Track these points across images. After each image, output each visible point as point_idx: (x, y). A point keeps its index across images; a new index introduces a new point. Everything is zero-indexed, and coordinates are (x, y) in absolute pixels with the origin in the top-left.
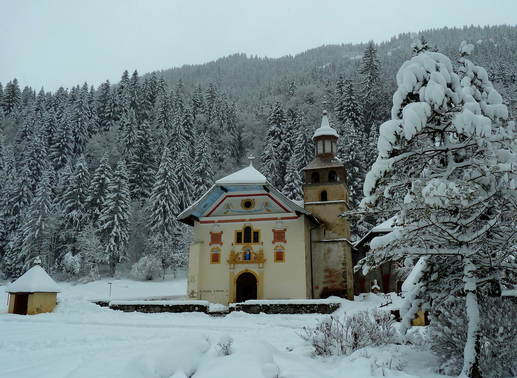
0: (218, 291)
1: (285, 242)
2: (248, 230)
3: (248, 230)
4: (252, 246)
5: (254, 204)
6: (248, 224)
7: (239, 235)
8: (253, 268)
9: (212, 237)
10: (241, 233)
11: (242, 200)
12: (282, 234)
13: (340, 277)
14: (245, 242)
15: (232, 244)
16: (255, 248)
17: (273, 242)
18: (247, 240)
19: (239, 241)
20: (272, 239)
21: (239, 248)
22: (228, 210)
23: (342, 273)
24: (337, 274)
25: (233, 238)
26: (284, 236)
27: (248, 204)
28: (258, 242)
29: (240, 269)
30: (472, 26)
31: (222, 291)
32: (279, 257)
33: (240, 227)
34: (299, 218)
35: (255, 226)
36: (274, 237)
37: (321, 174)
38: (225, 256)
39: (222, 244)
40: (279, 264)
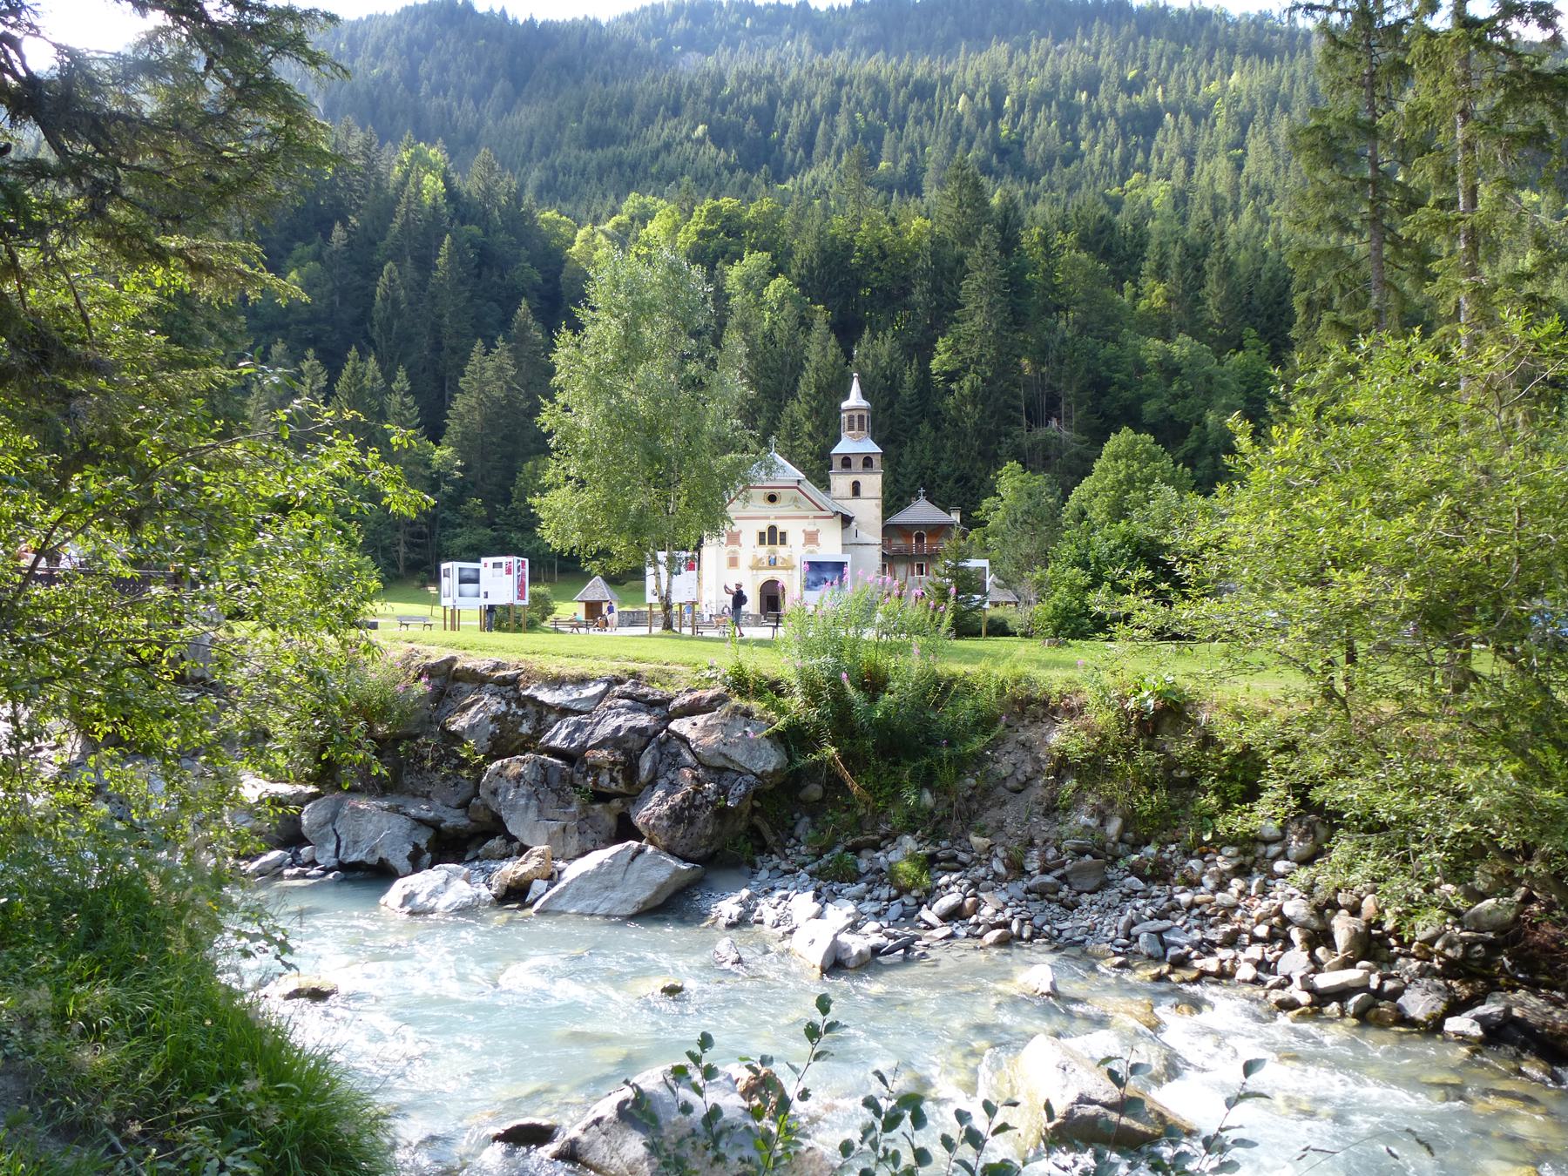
2: (772, 529)
3: (772, 529)
6: (773, 522)
7: (762, 534)
16: (781, 551)
18: (772, 541)
19: (762, 542)
21: (764, 551)
27: (772, 499)
33: (763, 526)
35: (781, 526)
37: (853, 460)
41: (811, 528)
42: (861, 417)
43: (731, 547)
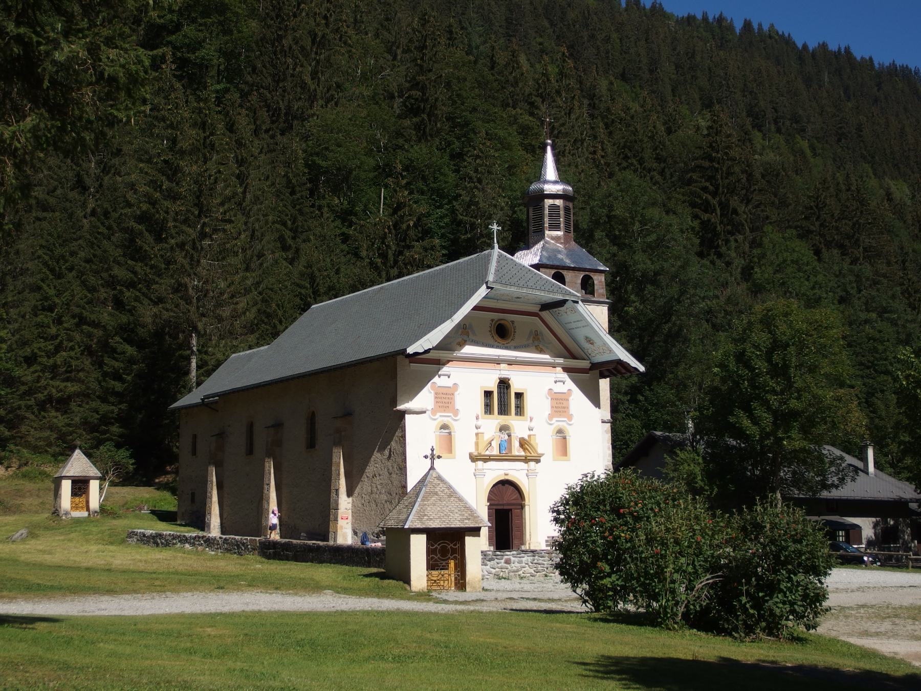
1: (570, 417)
2: (504, 384)
3: (504, 384)
4: (513, 422)
5: (515, 332)
7: (488, 394)
8: (516, 472)
9: (436, 398)
10: (492, 392)
11: (492, 320)
16: (519, 427)
17: (551, 417)
18: (504, 410)
19: (488, 408)
20: (548, 411)
22: (465, 337)
25: (479, 401)
29: (496, 472)
30: (824, 46)
33: (489, 379)
34: (590, 372)
35: (519, 380)
36: (552, 407)
39: (456, 412)
40: (562, 464)
41: (560, 388)
42: (567, 209)
43: (441, 418)
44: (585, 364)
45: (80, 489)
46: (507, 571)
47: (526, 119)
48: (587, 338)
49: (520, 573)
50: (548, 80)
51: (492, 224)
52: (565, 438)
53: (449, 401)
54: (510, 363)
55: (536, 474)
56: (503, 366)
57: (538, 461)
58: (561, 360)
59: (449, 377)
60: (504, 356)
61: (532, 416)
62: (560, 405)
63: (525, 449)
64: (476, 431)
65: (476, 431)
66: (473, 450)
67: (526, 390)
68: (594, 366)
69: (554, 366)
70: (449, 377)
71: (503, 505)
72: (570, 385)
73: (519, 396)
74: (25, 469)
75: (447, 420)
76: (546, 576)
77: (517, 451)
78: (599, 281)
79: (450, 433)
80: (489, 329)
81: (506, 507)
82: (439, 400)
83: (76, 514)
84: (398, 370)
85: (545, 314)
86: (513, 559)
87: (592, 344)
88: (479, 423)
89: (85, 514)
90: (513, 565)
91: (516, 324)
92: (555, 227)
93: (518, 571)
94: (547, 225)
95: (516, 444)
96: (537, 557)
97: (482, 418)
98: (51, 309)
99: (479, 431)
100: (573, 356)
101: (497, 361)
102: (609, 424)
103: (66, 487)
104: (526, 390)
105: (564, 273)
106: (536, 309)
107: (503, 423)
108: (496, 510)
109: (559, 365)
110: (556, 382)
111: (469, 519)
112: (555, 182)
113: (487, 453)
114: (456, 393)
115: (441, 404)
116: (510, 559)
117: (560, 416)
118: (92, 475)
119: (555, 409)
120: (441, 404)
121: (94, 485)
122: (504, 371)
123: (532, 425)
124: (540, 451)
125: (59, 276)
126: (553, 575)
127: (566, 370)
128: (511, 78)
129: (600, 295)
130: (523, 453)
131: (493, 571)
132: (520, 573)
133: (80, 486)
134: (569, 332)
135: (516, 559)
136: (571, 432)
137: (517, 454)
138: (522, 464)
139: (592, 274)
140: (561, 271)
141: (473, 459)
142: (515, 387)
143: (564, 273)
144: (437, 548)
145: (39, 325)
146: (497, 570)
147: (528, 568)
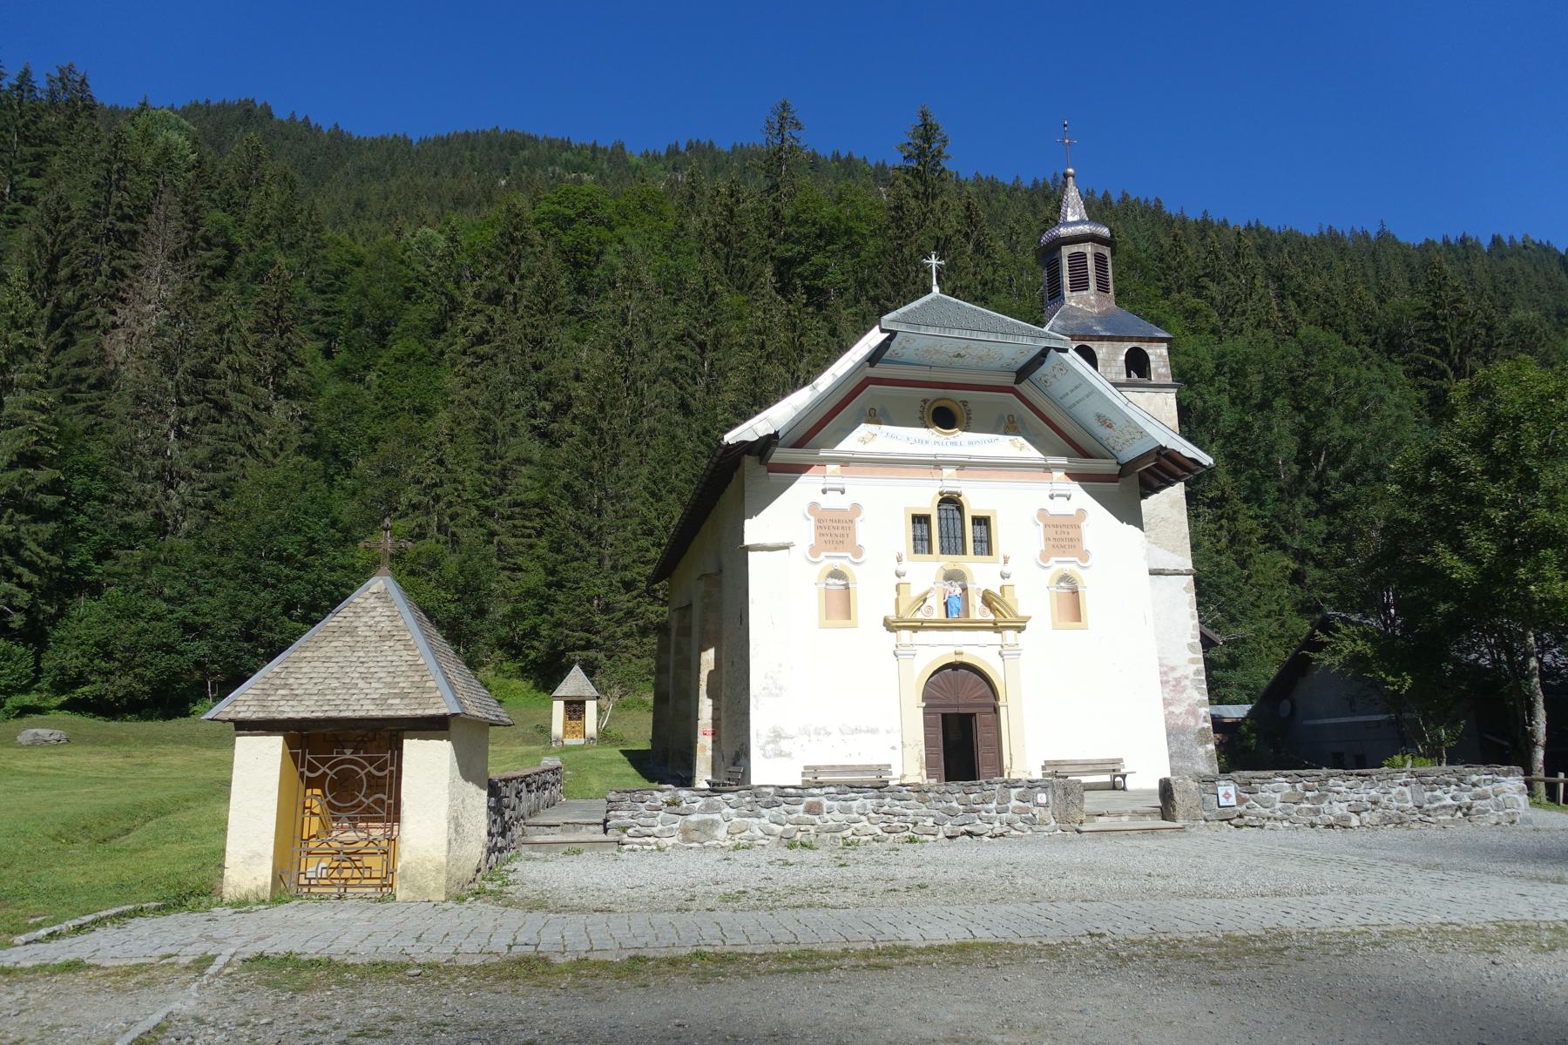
0: (857, 730)
1: (1085, 556)
2: (951, 502)
3: (951, 502)
7: (920, 520)
8: (979, 649)
9: (818, 527)
11: (925, 401)
12: (1070, 530)
13: (1185, 688)
14: (942, 552)
15: (899, 559)
16: (981, 573)
17: (1045, 556)
18: (954, 544)
19: (922, 543)
21: (927, 572)
23: (1192, 676)
24: (1176, 679)
25: (903, 533)
26: (1079, 540)
28: (990, 552)
29: (938, 649)
31: (873, 731)
32: (1072, 603)
33: (924, 495)
35: (978, 497)
36: (1047, 539)
38: (874, 600)
39: (858, 552)
41: (1060, 507)
42: (1100, 259)
43: (828, 562)
44: (1108, 466)
45: (575, 711)
46: (812, 830)
47: (1193, 302)
48: (1099, 417)
49: (845, 834)
50: (1217, 257)
51: (927, 256)
52: (1075, 592)
53: (844, 532)
54: (962, 465)
55: (1016, 651)
56: (948, 472)
57: (1020, 629)
58: (1064, 461)
59: (843, 492)
60: (945, 455)
61: (1006, 554)
62: (1063, 536)
63: (993, 610)
64: (898, 580)
65: (898, 580)
66: (891, 613)
67: (995, 511)
68: (1126, 469)
69: (1048, 469)
70: (843, 492)
71: (958, 706)
72: (1080, 498)
73: (982, 522)
74: (625, 698)
75: (838, 564)
76: (912, 840)
77: (978, 611)
78: (1158, 355)
79: (847, 587)
80: (919, 415)
81: (962, 711)
82: (823, 531)
83: (569, 741)
84: (747, 483)
85: (1024, 387)
86: (826, 803)
87: (1110, 426)
88: (901, 568)
89: (582, 741)
90: (827, 817)
91: (970, 405)
92: (1079, 284)
93: (839, 829)
94: (1066, 280)
95: (976, 602)
96: (888, 800)
97: (909, 560)
98: (650, 533)
99: (903, 579)
100: (1086, 455)
101: (937, 464)
102: (1191, 577)
103: (558, 708)
104: (995, 511)
105: (1094, 346)
106: (1009, 380)
107: (951, 567)
108: (944, 716)
109: (1058, 467)
110: (1052, 497)
111: (403, 695)
112: (1081, 222)
113: (919, 616)
114: (858, 520)
115: (829, 538)
116: (819, 804)
117: (1064, 554)
118: (587, 694)
119: (1052, 542)
120: (826, 538)
121: (591, 707)
122: (950, 481)
123: (1007, 569)
124: (1022, 612)
125: (659, 499)
126: (931, 838)
127: (1074, 476)
128: (1174, 263)
129: (1159, 375)
130: (992, 617)
131: (778, 829)
132: (845, 834)
133: (575, 708)
134: (1068, 413)
135: (835, 804)
136: (1088, 581)
137: (979, 617)
138: (991, 634)
139: (1144, 346)
140: (1088, 344)
141: (890, 626)
142: (974, 504)
143: (1094, 346)
144: (325, 774)
145: (639, 550)
146: (788, 826)
147: (867, 823)
